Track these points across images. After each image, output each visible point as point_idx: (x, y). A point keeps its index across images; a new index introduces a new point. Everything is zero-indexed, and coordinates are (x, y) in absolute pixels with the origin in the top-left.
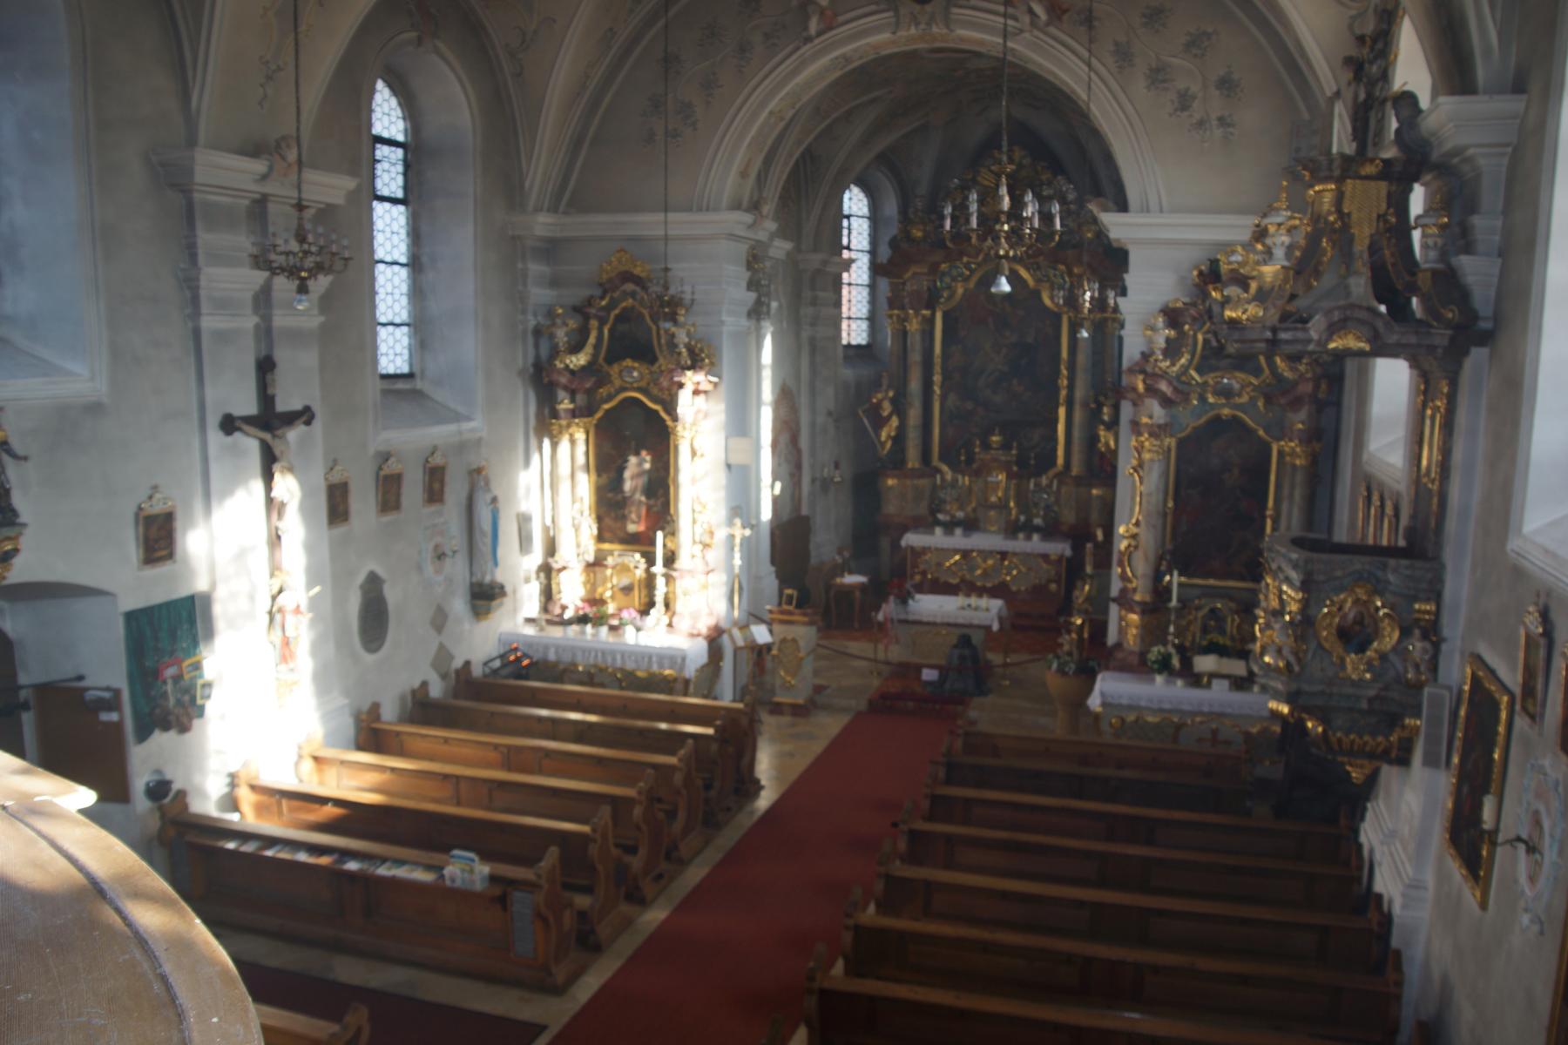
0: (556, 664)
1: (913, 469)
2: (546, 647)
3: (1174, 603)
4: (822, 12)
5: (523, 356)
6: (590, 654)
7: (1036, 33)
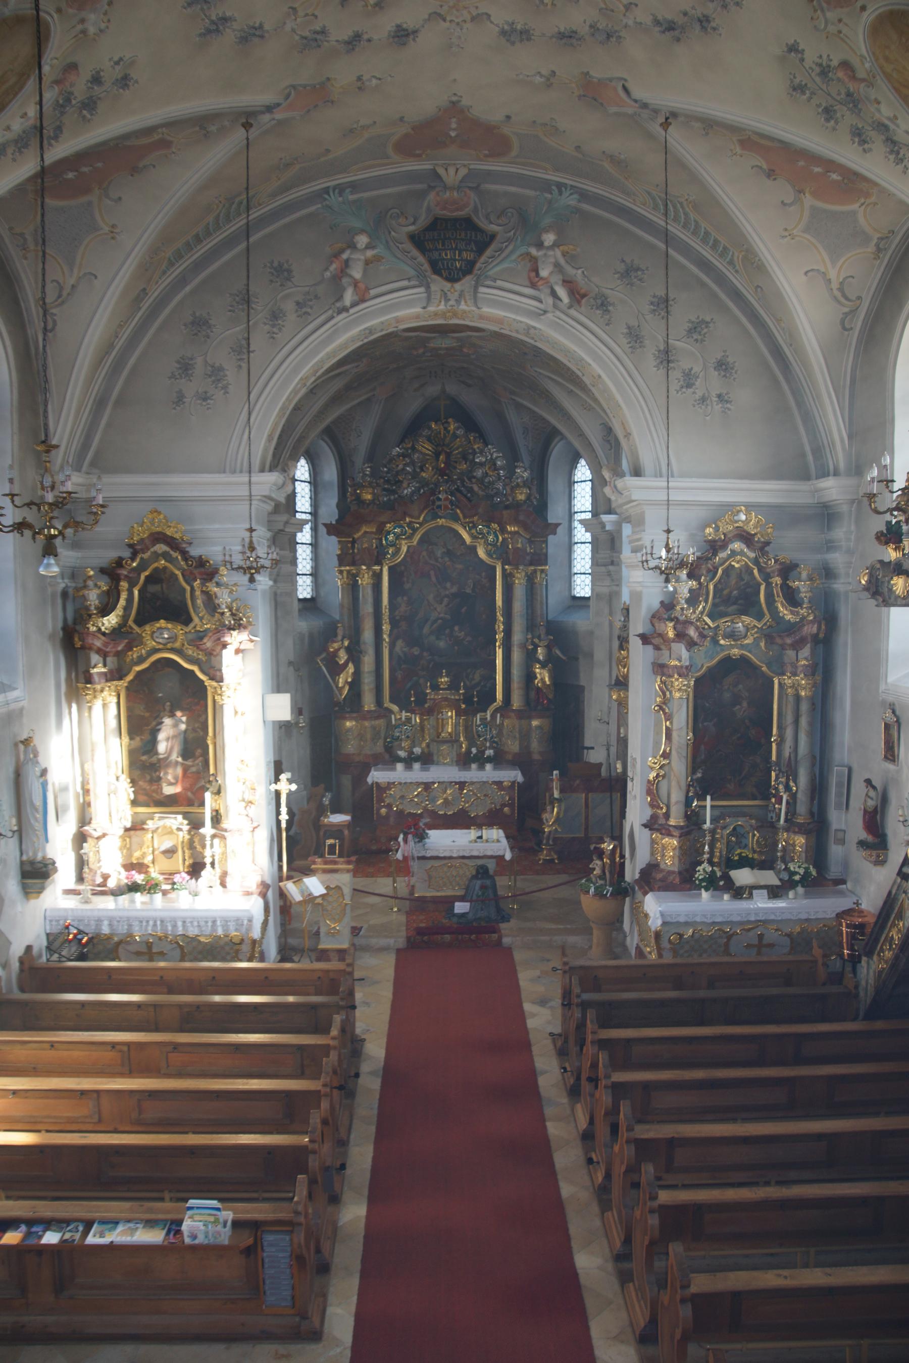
0: (109, 938)
1: (369, 712)
2: (99, 921)
3: (707, 825)
4: (356, 284)
5: (53, 620)
6: (148, 922)
7: (558, 313)
